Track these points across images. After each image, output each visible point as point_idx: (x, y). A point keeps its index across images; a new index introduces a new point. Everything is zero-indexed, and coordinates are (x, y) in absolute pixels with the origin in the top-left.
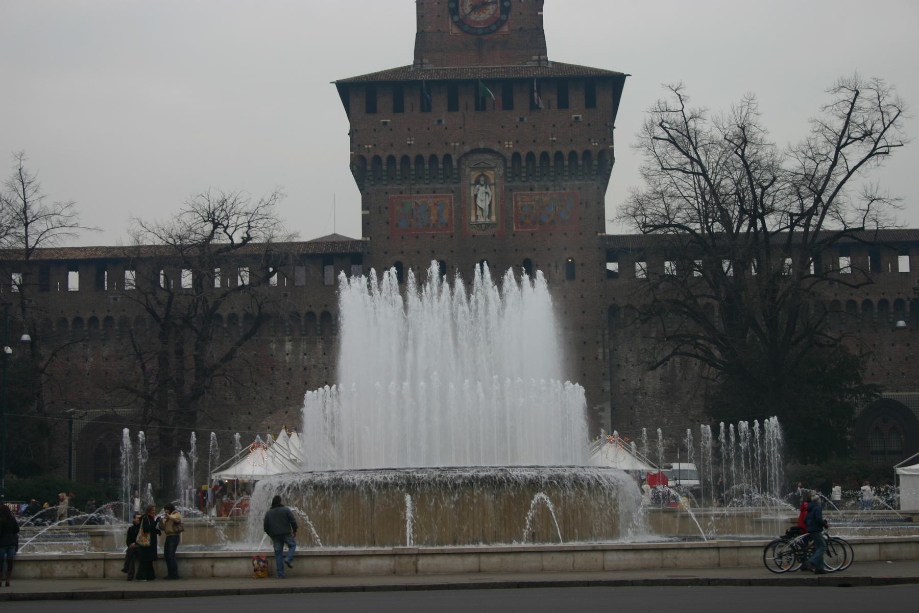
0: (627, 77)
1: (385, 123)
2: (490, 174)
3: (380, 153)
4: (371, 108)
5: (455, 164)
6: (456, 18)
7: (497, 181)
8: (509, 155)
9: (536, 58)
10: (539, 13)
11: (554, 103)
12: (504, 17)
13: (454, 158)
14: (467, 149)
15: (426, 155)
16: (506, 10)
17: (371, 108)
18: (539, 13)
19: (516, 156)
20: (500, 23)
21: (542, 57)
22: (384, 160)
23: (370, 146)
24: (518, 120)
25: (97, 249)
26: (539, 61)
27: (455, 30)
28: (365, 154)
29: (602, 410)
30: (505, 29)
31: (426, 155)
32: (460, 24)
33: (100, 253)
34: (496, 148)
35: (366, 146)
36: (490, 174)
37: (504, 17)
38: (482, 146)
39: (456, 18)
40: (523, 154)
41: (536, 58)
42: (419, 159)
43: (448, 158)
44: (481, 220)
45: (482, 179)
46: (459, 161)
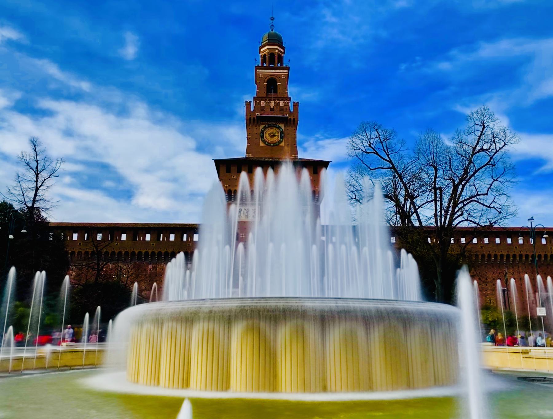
0: (330, 163)
1: (234, 177)
4: (228, 171)
6: (263, 139)
9: (294, 155)
10: (295, 139)
12: (281, 140)
16: (282, 137)
17: (228, 171)
18: (295, 139)
20: (280, 142)
21: (296, 156)
23: (227, 186)
25: (111, 224)
26: (295, 157)
27: (262, 144)
32: (264, 142)
33: (112, 225)
35: (226, 186)
37: (281, 140)
41: (294, 155)
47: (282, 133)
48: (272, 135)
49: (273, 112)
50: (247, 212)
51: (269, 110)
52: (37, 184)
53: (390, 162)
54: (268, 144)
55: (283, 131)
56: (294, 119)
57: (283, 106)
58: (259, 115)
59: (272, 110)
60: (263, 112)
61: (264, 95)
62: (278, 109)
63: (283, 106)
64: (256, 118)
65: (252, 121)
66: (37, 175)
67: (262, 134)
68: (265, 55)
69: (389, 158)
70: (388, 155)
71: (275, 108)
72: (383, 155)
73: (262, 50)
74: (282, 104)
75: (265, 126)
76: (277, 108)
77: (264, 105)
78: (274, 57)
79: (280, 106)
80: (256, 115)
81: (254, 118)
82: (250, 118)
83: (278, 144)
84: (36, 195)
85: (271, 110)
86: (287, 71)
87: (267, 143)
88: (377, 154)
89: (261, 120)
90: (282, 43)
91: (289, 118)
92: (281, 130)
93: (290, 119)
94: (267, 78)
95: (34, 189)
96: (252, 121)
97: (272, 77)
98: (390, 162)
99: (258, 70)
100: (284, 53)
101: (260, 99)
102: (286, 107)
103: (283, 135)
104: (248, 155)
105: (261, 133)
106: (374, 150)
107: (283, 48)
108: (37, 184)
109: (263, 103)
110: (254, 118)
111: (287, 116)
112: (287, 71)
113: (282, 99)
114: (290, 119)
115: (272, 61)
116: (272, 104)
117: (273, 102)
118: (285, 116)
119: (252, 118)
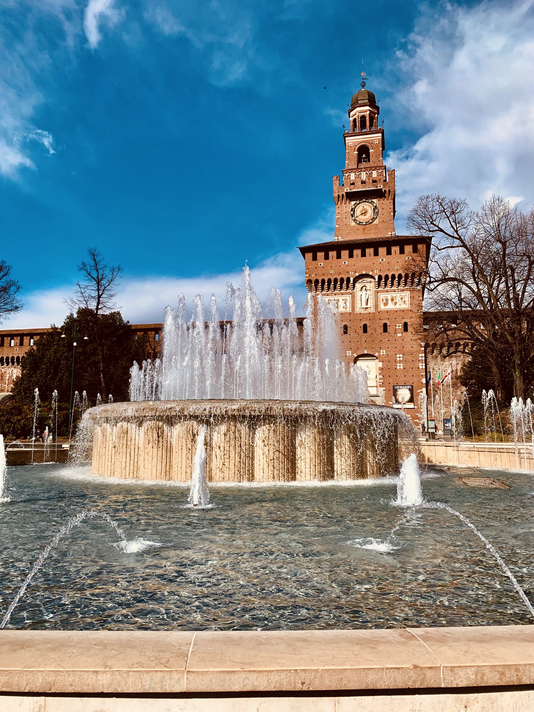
2: (368, 285)
3: (318, 278)
5: (352, 281)
6: (353, 218)
7: (371, 289)
8: (377, 277)
11: (398, 252)
13: (352, 279)
14: (357, 274)
15: (339, 278)
19: (380, 277)
20: (373, 219)
22: (320, 281)
24: (381, 260)
27: (353, 224)
28: (312, 279)
29: (422, 392)
30: (376, 222)
31: (339, 278)
34: (371, 273)
36: (368, 285)
38: (364, 273)
39: (353, 218)
40: (383, 276)
41: (390, 233)
42: (336, 280)
43: (348, 279)
44: (364, 306)
45: (364, 288)
46: (353, 280)
47: (376, 208)
48: (364, 211)
49: (364, 185)
50: (337, 303)
51: (360, 183)
52: (99, 292)
53: (460, 239)
54: (360, 223)
55: (376, 207)
56: (389, 190)
57: (376, 176)
58: (349, 191)
59: (363, 182)
60: (352, 186)
61: (355, 167)
62: (371, 181)
63: (376, 176)
64: (345, 194)
65: (341, 198)
66: (98, 283)
67: (352, 213)
68: (355, 120)
69: (458, 234)
70: (457, 232)
71: (367, 180)
72: (450, 231)
73: (351, 114)
74: (375, 174)
75: (356, 203)
76: (369, 179)
77: (354, 178)
78: (365, 121)
79: (373, 176)
80: (345, 191)
81: (343, 195)
82: (339, 195)
83: (371, 221)
84: (98, 304)
85: (362, 183)
86: (380, 135)
87: (358, 222)
88: (442, 230)
89: (351, 196)
90: (375, 102)
91: (383, 190)
92: (375, 205)
93: (385, 190)
94: (358, 146)
95: (97, 297)
96: (341, 198)
97: (363, 143)
98: (460, 239)
99: (347, 139)
100: (378, 113)
101: (350, 171)
102: (380, 177)
103: (376, 211)
104: (337, 238)
105: (352, 210)
106: (439, 228)
107: (377, 108)
108: (99, 292)
109: (353, 176)
110: (343, 195)
111: (382, 187)
112: (380, 135)
113: (375, 168)
114: (385, 190)
115: (363, 125)
116: (364, 176)
117: (364, 173)
118: (379, 188)
119: (341, 195)
